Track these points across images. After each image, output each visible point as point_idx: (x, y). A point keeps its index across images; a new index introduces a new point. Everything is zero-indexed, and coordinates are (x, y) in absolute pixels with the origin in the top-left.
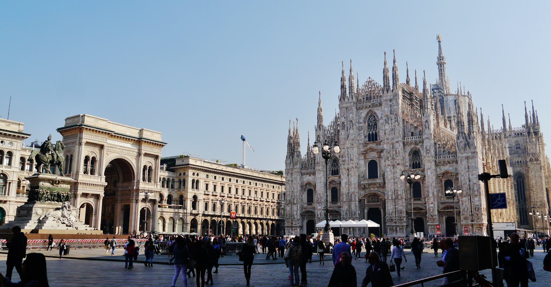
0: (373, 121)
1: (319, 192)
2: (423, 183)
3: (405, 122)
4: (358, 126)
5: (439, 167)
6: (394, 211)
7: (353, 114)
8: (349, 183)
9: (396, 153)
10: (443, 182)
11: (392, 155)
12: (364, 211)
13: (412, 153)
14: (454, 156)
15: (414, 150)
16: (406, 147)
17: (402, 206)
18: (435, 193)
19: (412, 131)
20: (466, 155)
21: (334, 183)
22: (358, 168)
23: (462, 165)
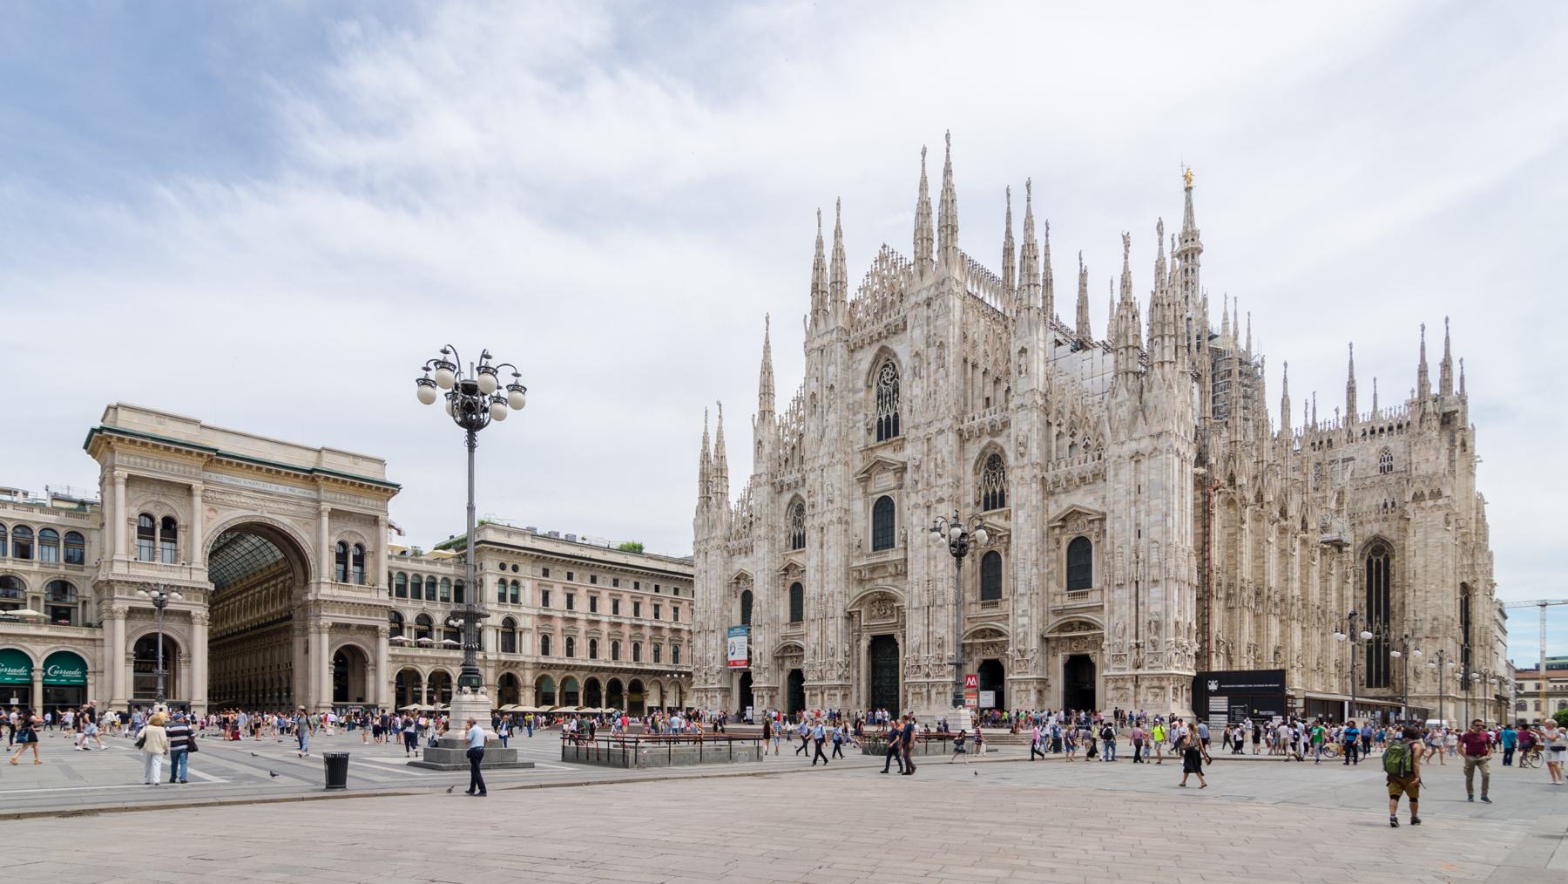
1: (760, 597)
2: (1007, 555)
3: (969, 366)
5: (1056, 497)
8: (822, 568)
9: (936, 465)
10: (1064, 546)
11: (926, 475)
12: (859, 646)
13: (984, 463)
14: (1099, 458)
15: (989, 452)
17: (945, 626)
18: (1034, 582)
19: (987, 395)
20: (1134, 446)
22: (847, 522)
23: (1119, 483)
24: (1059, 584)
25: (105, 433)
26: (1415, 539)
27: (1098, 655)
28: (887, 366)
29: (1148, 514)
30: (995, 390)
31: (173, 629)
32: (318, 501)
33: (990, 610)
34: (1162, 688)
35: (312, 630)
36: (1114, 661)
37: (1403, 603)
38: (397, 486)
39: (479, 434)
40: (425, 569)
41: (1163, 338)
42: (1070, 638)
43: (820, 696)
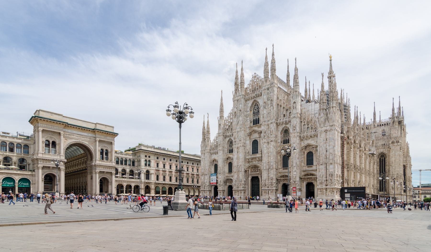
0: (257, 109)
1: (220, 166)
3: (279, 106)
4: (246, 114)
5: (303, 141)
6: (268, 178)
7: (242, 105)
8: (238, 158)
9: (270, 132)
10: (306, 154)
11: (267, 134)
13: (283, 131)
14: (316, 131)
15: (285, 129)
16: (279, 127)
17: (273, 174)
20: (325, 128)
21: (230, 159)
22: (245, 146)
23: (321, 138)
24: (304, 164)
25: (36, 118)
26: (392, 153)
27: (315, 182)
28: (256, 105)
29: (329, 146)
30: (286, 112)
31: (55, 172)
32: (95, 138)
33: (285, 170)
34: (333, 191)
35: (94, 173)
36: (320, 184)
37: (389, 170)
38: (117, 134)
39: (182, 124)
40: (124, 157)
41: (333, 100)
42: (308, 178)
43: (237, 192)
